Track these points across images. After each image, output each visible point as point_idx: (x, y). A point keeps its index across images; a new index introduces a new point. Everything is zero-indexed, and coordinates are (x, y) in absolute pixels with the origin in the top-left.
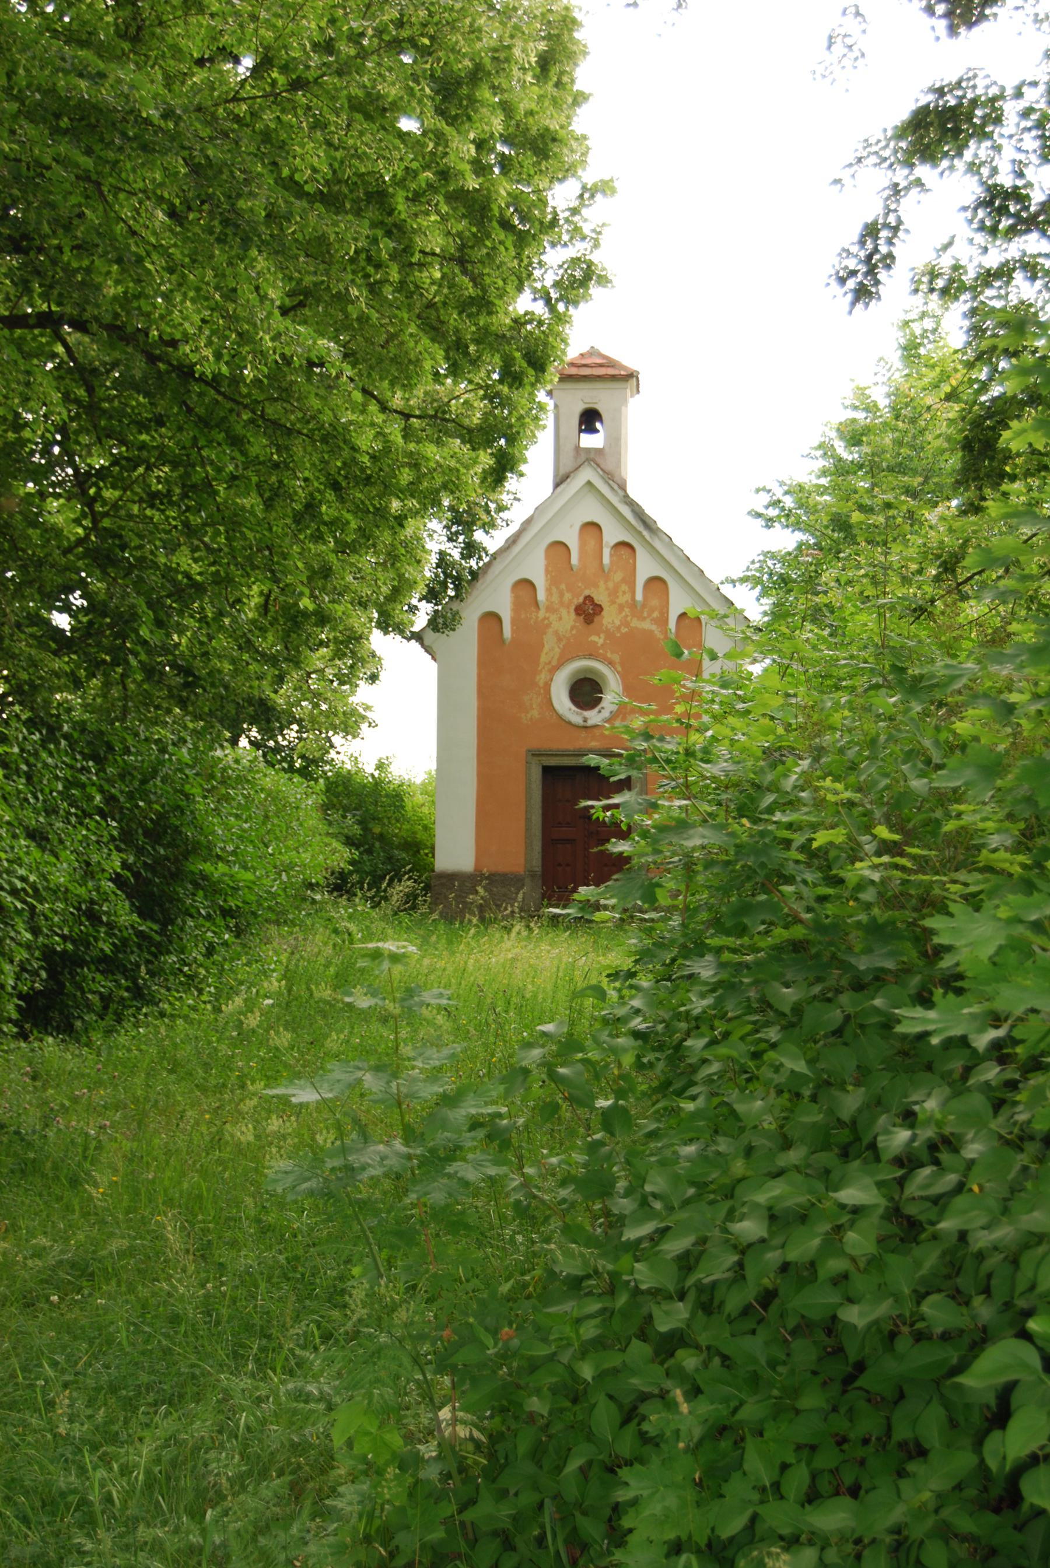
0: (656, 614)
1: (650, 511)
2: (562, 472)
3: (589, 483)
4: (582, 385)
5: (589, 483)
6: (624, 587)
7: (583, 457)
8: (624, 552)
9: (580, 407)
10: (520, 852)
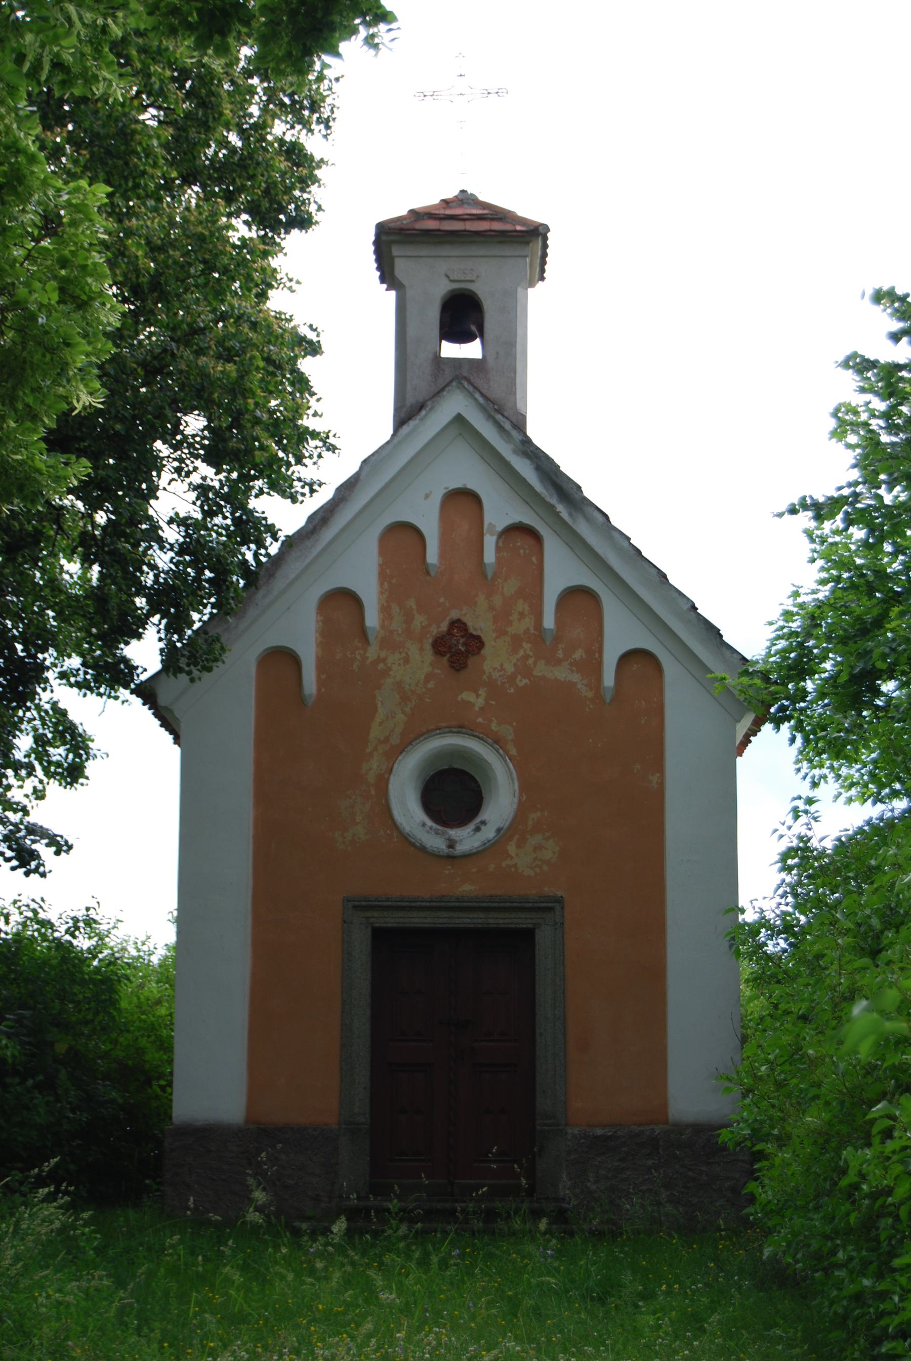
0: (579, 654)
1: (568, 468)
2: (410, 400)
3: (459, 419)
4: (445, 251)
5: (459, 419)
6: (521, 606)
7: (448, 374)
8: (521, 542)
9: (441, 289)
10: (325, 1092)
